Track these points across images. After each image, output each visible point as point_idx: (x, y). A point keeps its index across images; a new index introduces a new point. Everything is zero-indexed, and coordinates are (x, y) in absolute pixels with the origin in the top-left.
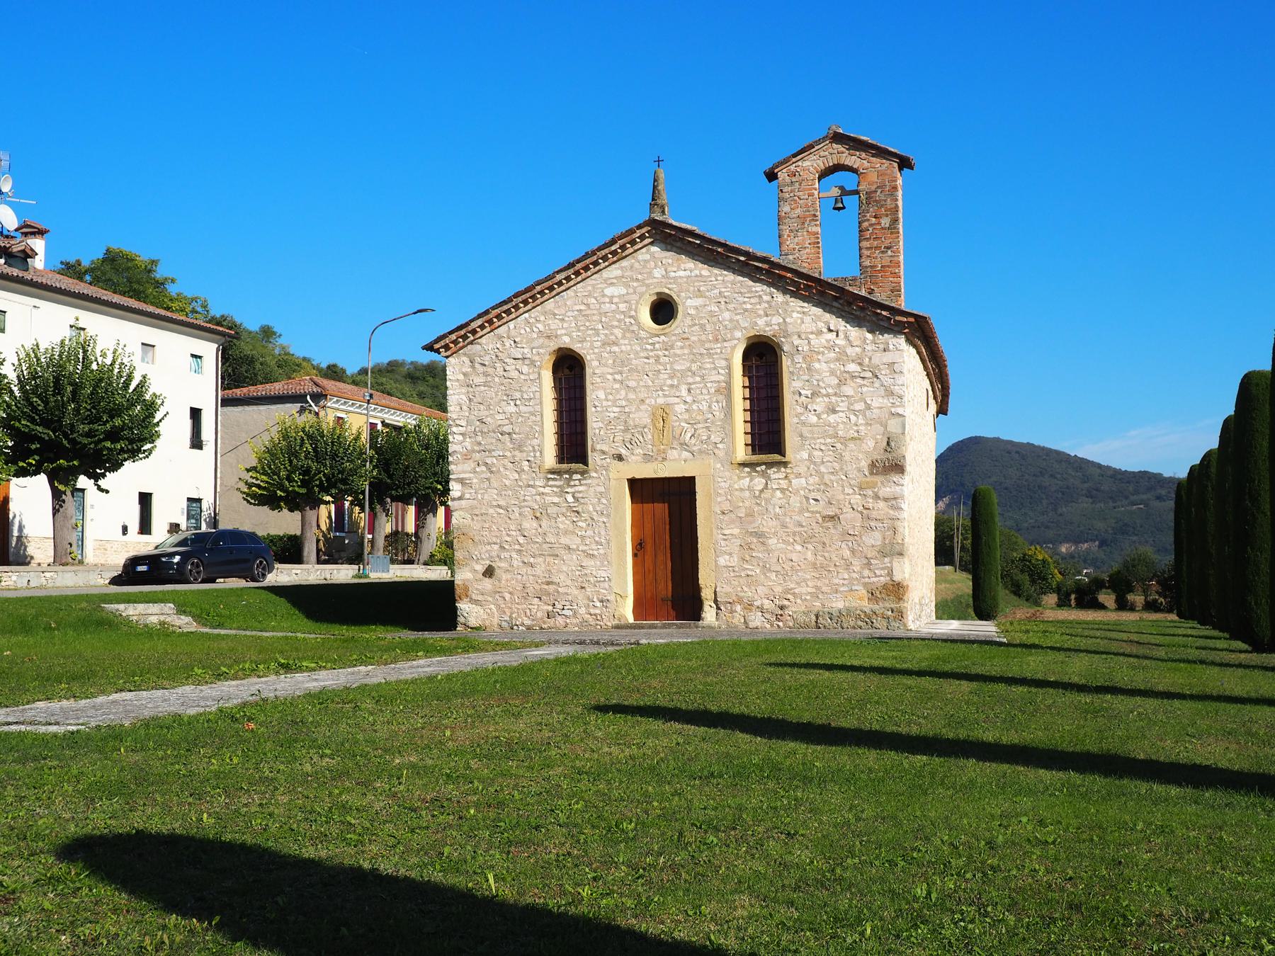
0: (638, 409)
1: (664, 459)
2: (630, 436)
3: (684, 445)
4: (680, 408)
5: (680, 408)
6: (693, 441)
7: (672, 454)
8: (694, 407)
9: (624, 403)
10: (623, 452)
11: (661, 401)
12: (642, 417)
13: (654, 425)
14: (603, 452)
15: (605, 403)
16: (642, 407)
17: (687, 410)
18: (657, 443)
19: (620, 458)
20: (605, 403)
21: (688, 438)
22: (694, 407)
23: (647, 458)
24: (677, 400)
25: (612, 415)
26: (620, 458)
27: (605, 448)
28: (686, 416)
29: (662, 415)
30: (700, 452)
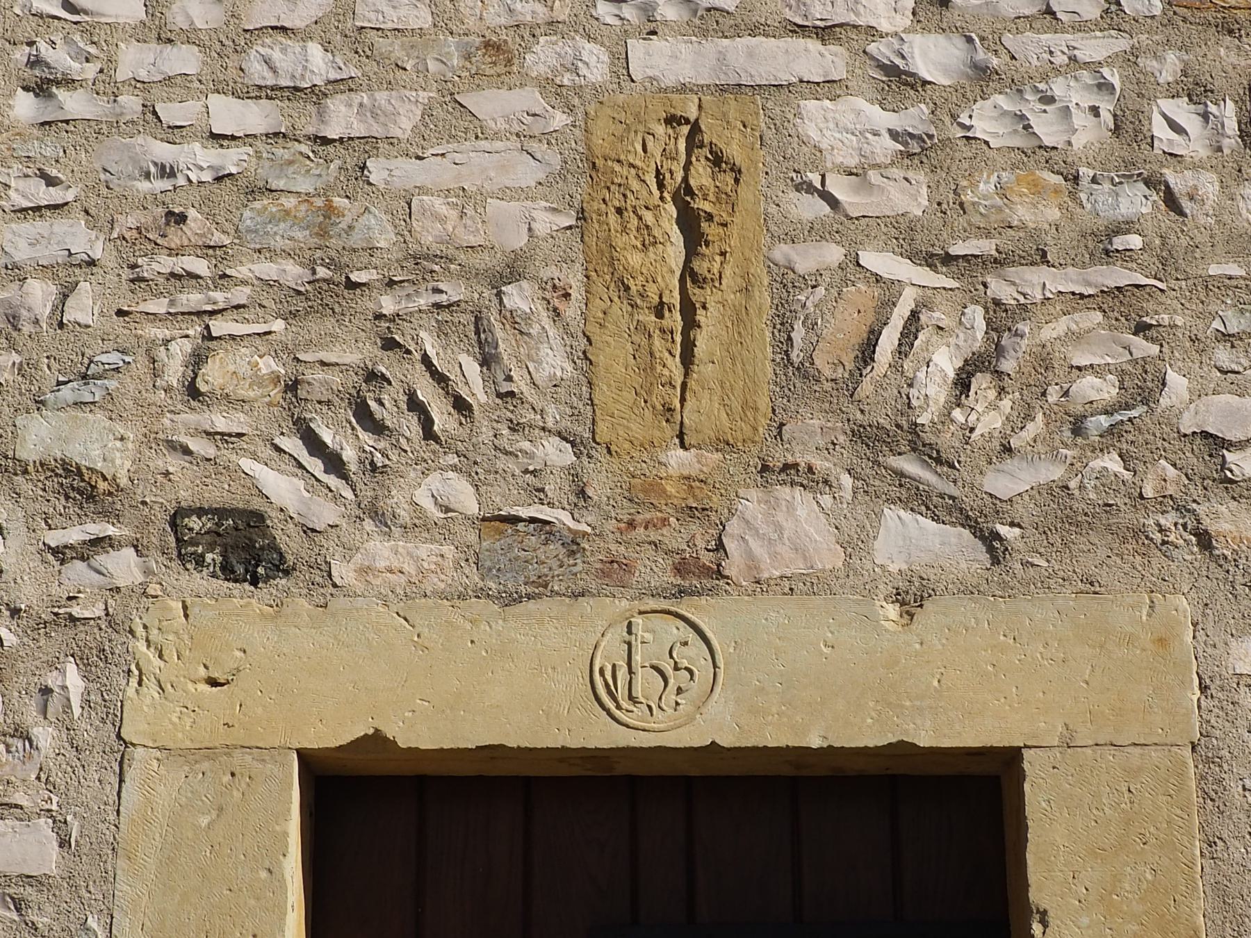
0: (451, 119)
1: (702, 573)
2: (353, 351)
3: (896, 454)
4: (849, 126)
5: (849, 126)
6: (988, 414)
7: (785, 528)
8: (986, 120)
9: (318, 64)
10: (281, 488)
11: (670, 61)
12: (491, 187)
13: (608, 271)
14: (80, 487)
15: (135, 60)
16: (491, 104)
17: (915, 150)
18: (625, 420)
19: (243, 547)
20: (135, 60)
21: (933, 387)
22: (986, 120)
23: (519, 558)
24: (813, 59)
25: (199, 159)
26: (243, 547)
27: (101, 446)
28: (909, 196)
29: (684, 184)
30: (1064, 514)
